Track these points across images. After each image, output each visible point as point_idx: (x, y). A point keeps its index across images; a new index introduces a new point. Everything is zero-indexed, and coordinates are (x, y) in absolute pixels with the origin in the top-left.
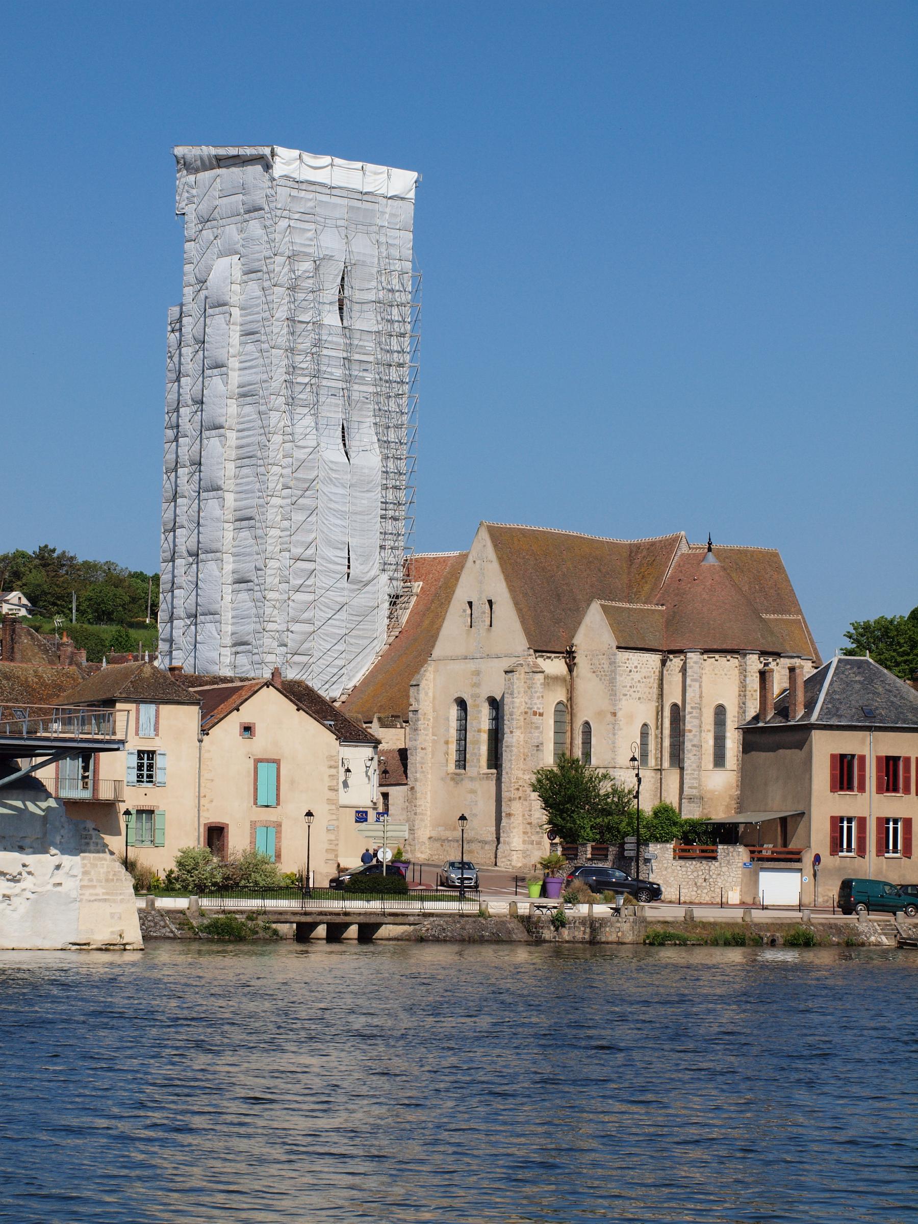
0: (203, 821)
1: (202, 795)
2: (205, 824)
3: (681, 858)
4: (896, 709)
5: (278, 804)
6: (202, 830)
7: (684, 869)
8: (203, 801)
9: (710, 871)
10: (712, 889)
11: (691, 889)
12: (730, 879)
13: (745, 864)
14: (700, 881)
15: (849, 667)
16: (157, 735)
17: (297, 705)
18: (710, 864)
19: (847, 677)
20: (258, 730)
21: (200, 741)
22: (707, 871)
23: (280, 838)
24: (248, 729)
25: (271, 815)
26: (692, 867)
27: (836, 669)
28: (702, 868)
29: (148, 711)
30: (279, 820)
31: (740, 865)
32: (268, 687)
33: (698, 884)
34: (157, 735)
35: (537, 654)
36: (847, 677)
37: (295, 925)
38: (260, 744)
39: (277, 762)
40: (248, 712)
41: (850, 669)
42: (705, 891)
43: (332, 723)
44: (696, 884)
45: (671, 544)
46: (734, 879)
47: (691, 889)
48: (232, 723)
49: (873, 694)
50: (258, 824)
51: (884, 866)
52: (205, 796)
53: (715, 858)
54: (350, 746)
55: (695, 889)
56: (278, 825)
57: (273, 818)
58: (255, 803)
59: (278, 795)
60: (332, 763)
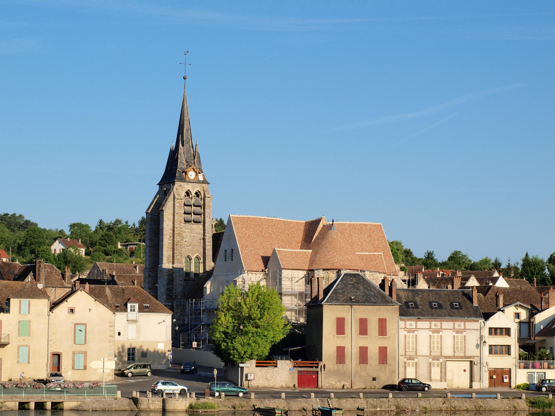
0: (50, 351)
1: (49, 339)
2: (51, 353)
3: (257, 366)
4: (367, 296)
5: (85, 343)
6: (49, 355)
7: (261, 372)
8: (50, 343)
9: (273, 372)
10: (275, 381)
11: (264, 381)
12: (283, 376)
13: (290, 369)
14: (268, 377)
15: (349, 277)
16: (29, 313)
17: (95, 299)
18: (273, 369)
19: (347, 282)
20: (77, 311)
21: (48, 316)
22: (272, 373)
23: (86, 358)
24: (72, 311)
25: (83, 348)
26: (265, 371)
27: (342, 278)
28: (270, 371)
29: (25, 301)
30: (86, 351)
31: (288, 369)
32: (81, 291)
33: (268, 379)
34: (29, 313)
35: (249, 272)
36: (347, 282)
37: (18, 403)
38: (76, 317)
39: (86, 324)
40: (72, 302)
41: (349, 278)
42: (271, 382)
43: (149, 305)
44: (266, 378)
45: (318, 222)
46: (285, 376)
47: (264, 381)
48: (63, 308)
49: (357, 289)
50: (76, 353)
51: (359, 369)
52: (51, 340)
53: (276, 366)
54: (155, 315)
55: (266, 381)
56: (85, 353)
57: (83, 350)
58: (75, 343)
59: (85, 339)
60: (111, 325)
